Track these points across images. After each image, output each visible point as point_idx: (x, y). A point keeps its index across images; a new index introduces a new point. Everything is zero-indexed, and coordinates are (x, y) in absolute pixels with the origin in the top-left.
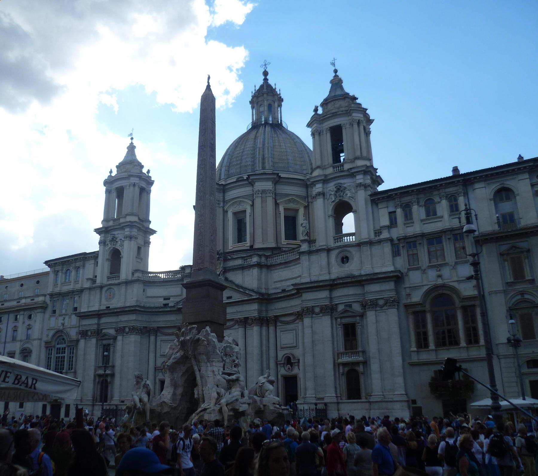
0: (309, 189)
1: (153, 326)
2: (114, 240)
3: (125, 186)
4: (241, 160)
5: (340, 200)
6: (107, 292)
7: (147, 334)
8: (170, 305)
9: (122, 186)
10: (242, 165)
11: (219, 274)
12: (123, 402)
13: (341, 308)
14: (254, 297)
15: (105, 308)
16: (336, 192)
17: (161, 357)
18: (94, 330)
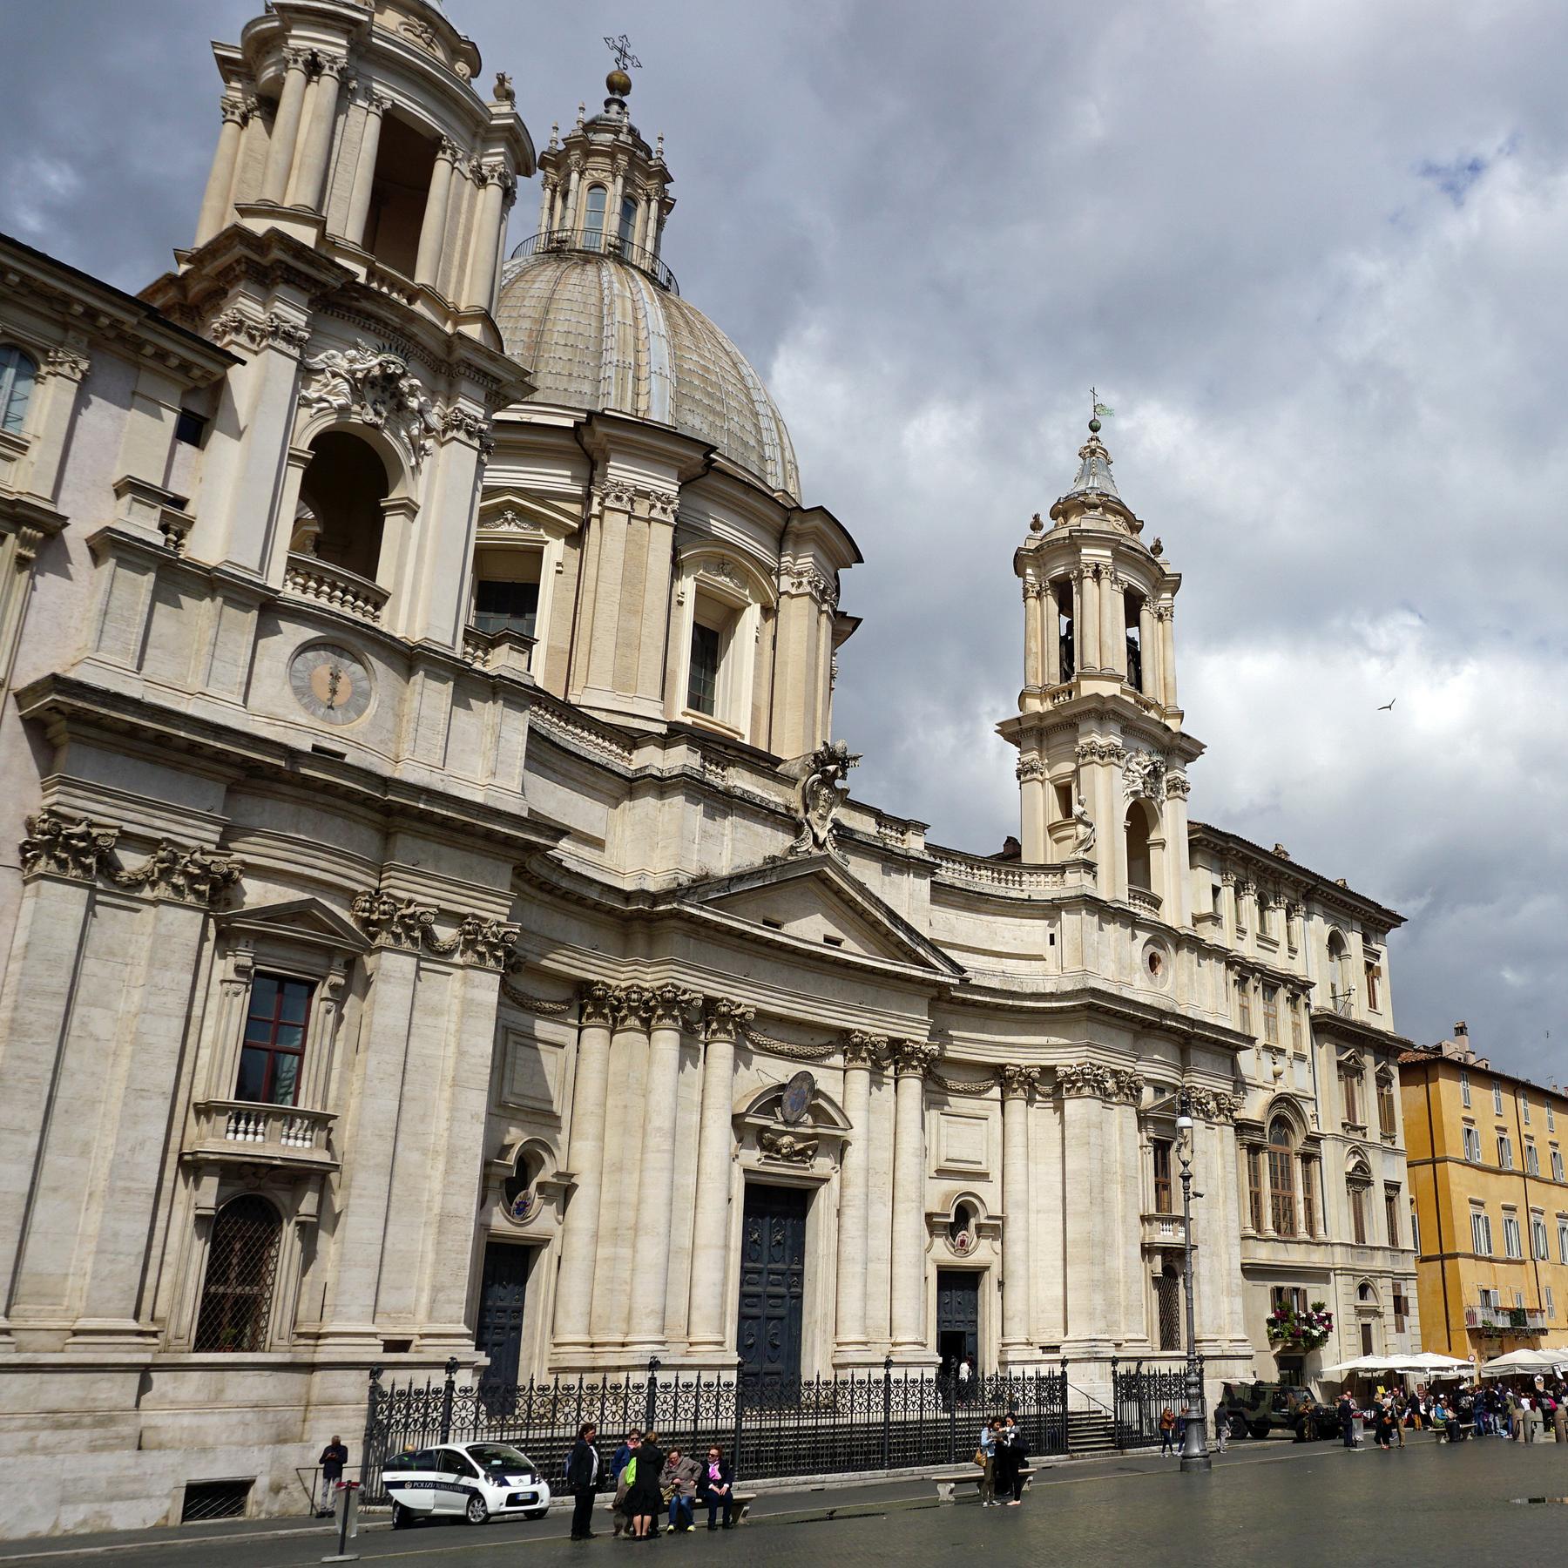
6: (310, 655)
13: (1148, 1094)
18: (204, 852)
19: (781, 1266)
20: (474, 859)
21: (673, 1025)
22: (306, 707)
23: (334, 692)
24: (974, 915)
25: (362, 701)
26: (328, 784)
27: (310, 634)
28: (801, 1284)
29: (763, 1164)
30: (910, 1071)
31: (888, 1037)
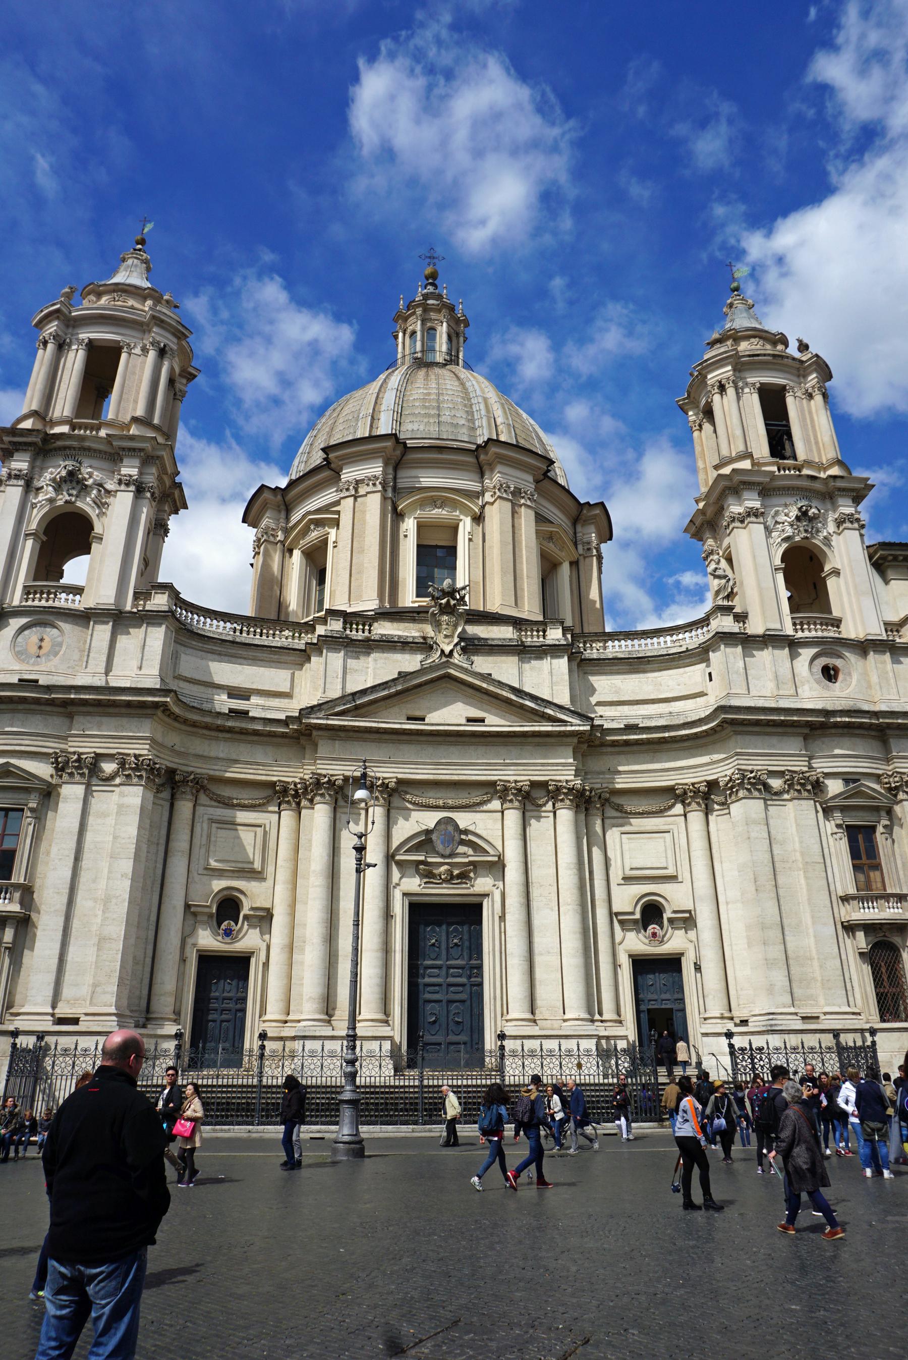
0: (579, 528)
1: (191, 769)
2: (72, 479)
3: (128, 345)
4: (438, 408)
5: (807, 538)
6: (26, 632)
7: (166, 794)
8: (251, 714)
9: (119, 342)
10: (443, 419)
11: (451, 652)
12: (61, 1021)
13: (834, 787)
14: (577, 728)
15: (16, 681)
16: (798, 518)
17: (205, 872)
19: (459, 962)
20: (124, 721)
21: (322, 800)
22: (23, 661)
23: (40, 647)
24: (641, 675)
25: (57, 648)
26: (19, 697)
27: (23, 621)
28: (480, 975)
29: (424, 888)
30: (560, 804)
31: (530, 781)
